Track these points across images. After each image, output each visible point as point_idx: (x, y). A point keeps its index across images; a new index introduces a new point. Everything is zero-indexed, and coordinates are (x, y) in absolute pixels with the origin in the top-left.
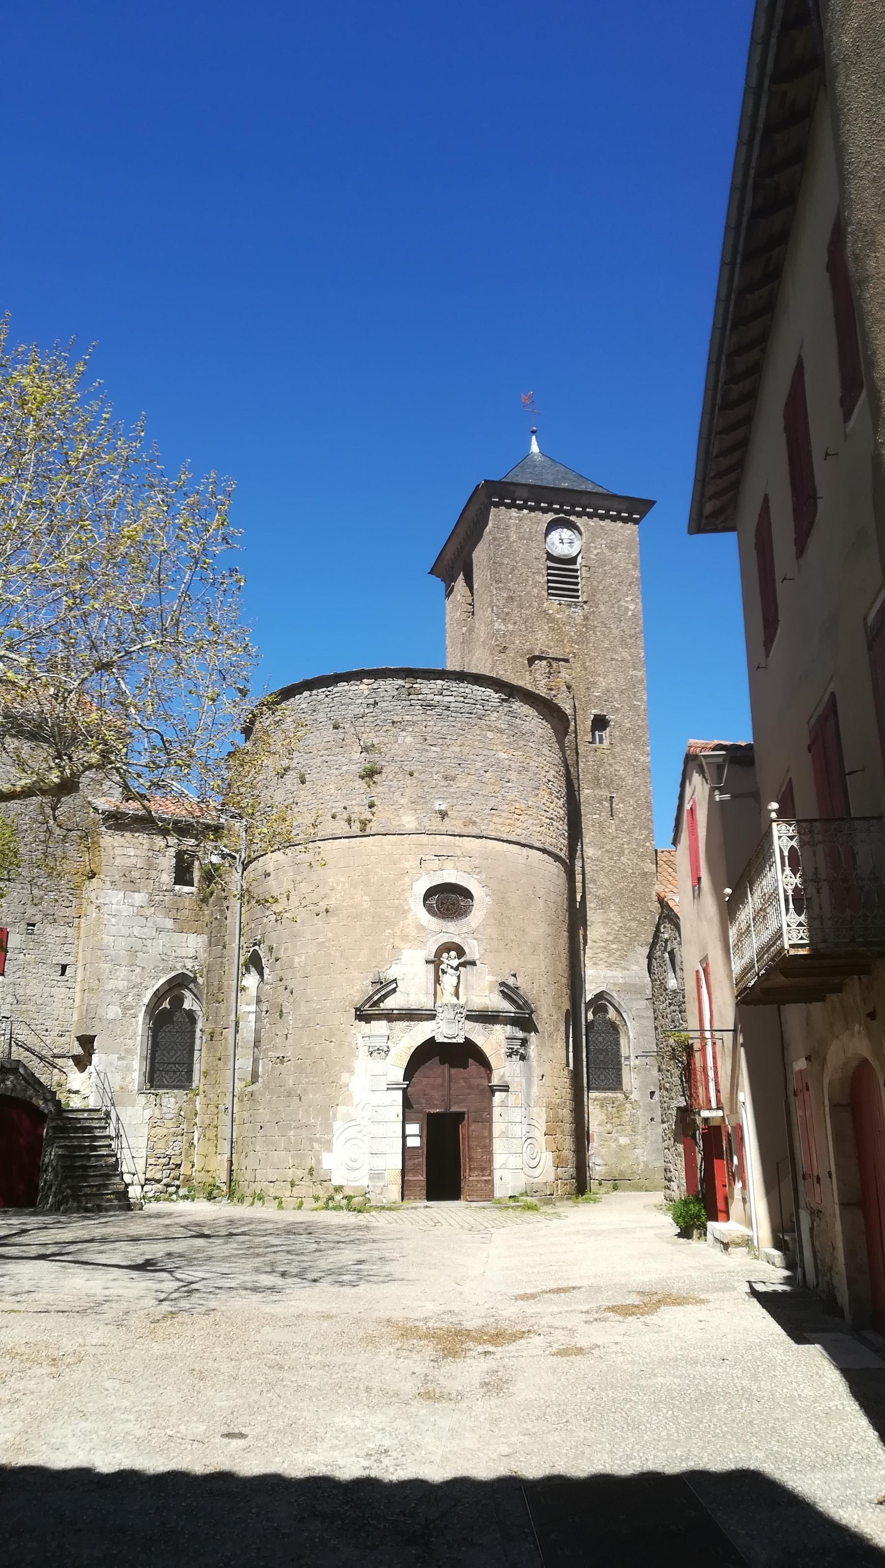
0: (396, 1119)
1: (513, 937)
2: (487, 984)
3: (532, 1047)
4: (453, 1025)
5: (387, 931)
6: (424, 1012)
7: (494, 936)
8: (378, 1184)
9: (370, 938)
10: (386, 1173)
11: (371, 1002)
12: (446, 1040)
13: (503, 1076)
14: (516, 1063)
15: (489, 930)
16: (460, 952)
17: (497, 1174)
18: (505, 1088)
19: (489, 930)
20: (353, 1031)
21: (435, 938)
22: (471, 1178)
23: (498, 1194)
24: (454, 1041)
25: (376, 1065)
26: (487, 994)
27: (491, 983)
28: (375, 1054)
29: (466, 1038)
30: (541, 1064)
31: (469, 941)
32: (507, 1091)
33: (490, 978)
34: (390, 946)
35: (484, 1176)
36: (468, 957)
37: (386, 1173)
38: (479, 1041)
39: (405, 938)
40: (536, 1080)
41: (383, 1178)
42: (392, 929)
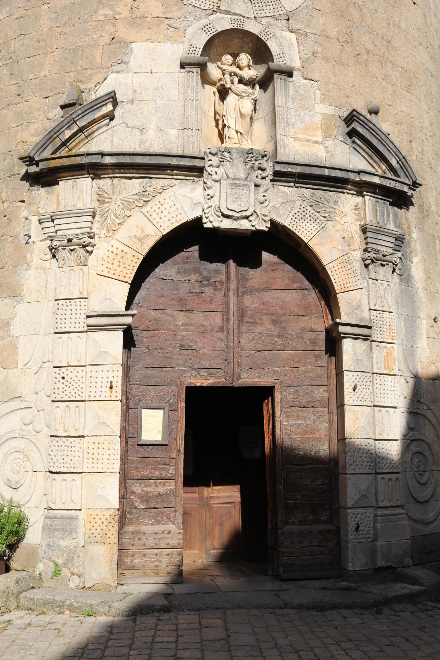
0: (106, 394)
1: (371, 47)
2: (318, 119)
3: (416, 260)
4: (244, 191)
5: (102, 12)
6: (175, 162)
7: (333, 32)
8: (63, 543)
9: (66, 30)
10: (81, 515)
11: (58, 142)
12: (226, 224)
13: (359, 307)
14: (387, 285)
15: (321, 20)
16: (260, 51)
17: (352, 517)
18: (364, 332)
19: (321, 20)
20: (25, 213)
21: (204, 21)
22: (287, 527)
23: (355, 562)
24: (245, 225)
25: (66, 277)
26: (320, 138)
27: (327, 118)
28: (61, 254)
29: (272, 222)
30: (432, 296)
31: (279, 33)
32: (367, 338)
33: (322, 109)
34: (106, 39)
35: (317, 522)
36: (278, 62)
37: (81, 515)
38: (305, 231)
39: (137, 20)
40: (424, 324)
41: (73, 531)
42: (112, 8)
